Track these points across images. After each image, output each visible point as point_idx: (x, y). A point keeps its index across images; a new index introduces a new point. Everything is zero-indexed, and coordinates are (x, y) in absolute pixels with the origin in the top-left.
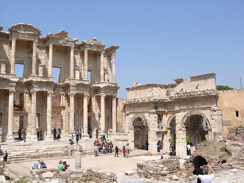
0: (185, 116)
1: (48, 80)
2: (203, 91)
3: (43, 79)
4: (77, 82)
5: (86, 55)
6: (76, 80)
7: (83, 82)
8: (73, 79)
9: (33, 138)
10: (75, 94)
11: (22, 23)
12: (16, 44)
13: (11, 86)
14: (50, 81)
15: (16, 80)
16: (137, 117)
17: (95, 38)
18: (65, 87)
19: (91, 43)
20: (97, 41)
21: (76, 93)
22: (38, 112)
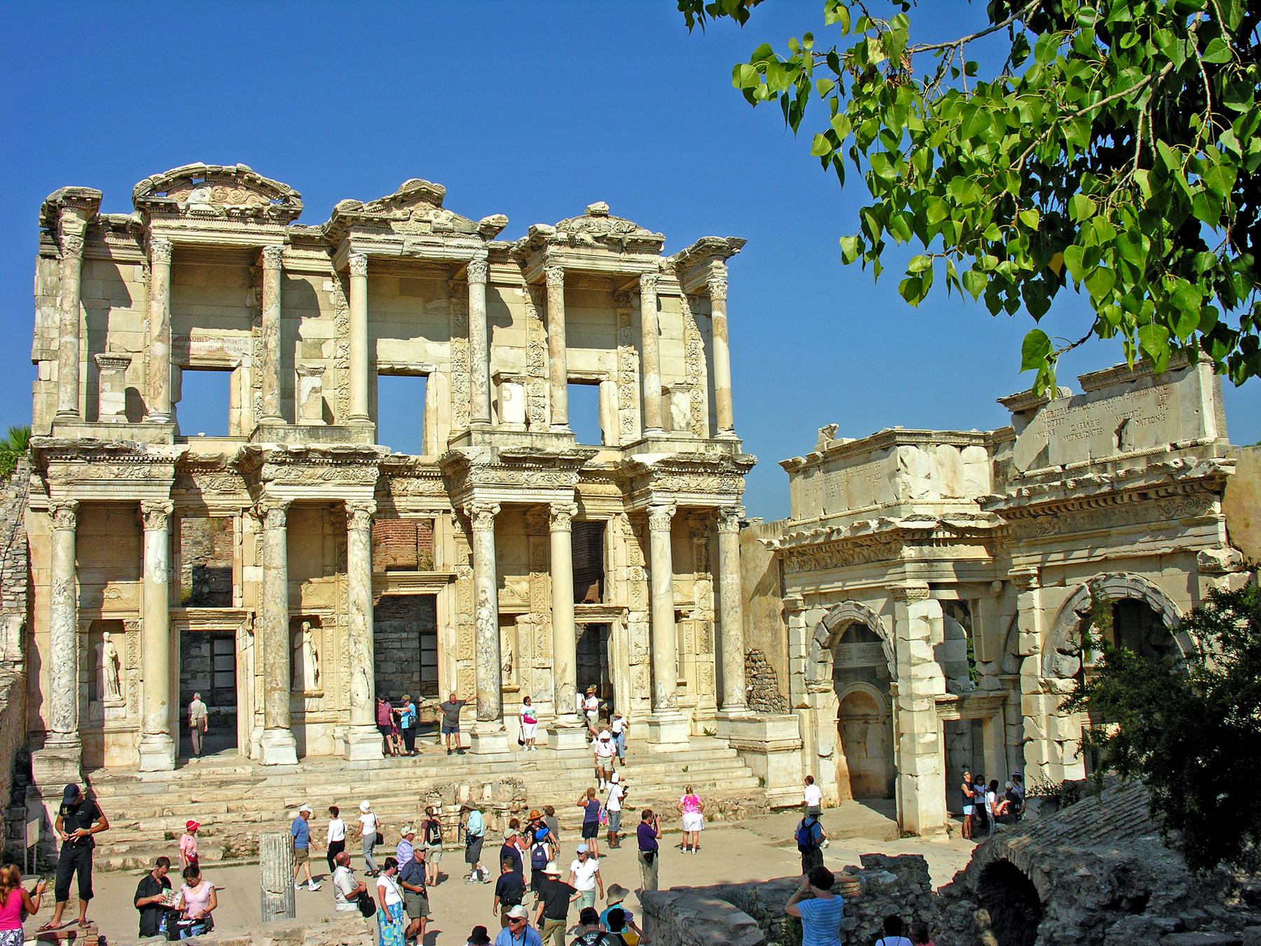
0: (1064, 607)
1: (344, 445)
2: (1149, 457)
3: (317, 438)
5: (556, 297)
6: (503, 433)
7: (538, 444)
8: (484, 432)
9: (274, 746)
10: (497, 510)
11: (200, 164)
12: (173, 268)
14: (353, 446)
15: (175, 451)
16: (836, 621)
17: (599, 206)
18: (449, 472)
19: (582, 235)
21: (502, 505)
22: (314, 612)
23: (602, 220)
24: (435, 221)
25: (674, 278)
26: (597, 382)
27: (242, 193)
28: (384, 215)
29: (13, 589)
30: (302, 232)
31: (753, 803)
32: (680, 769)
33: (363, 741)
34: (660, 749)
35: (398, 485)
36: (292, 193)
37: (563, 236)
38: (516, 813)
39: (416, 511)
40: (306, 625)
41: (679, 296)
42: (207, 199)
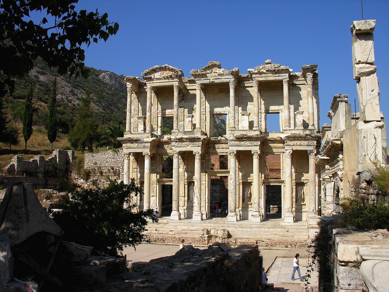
4: (238, 134)
8: (232, 131)
9: (173, 215)
10: (235, 153)
11: (157, 66)
13: (144, 147)
14: (193, 136)
15: (150, 139)
17: (267, 61)
20: (272, 65)
23: (269, 65)
24: (218, 72)
25: (303, 79)
26: (278, 113)
27: (168, 72)
28: (203, 73)
29: (122, 173)
30: (190, 79)
31: (302, 243)
32: (286, 231)
33: (195, 215)
34: (284, 224)
35: (217, 146)
36: (178, 70)
37: (256, 71)
38: (224, 238)
39: (223, 153)
40: (192, 184)
41: (305, 84)
42: (159, 75)
